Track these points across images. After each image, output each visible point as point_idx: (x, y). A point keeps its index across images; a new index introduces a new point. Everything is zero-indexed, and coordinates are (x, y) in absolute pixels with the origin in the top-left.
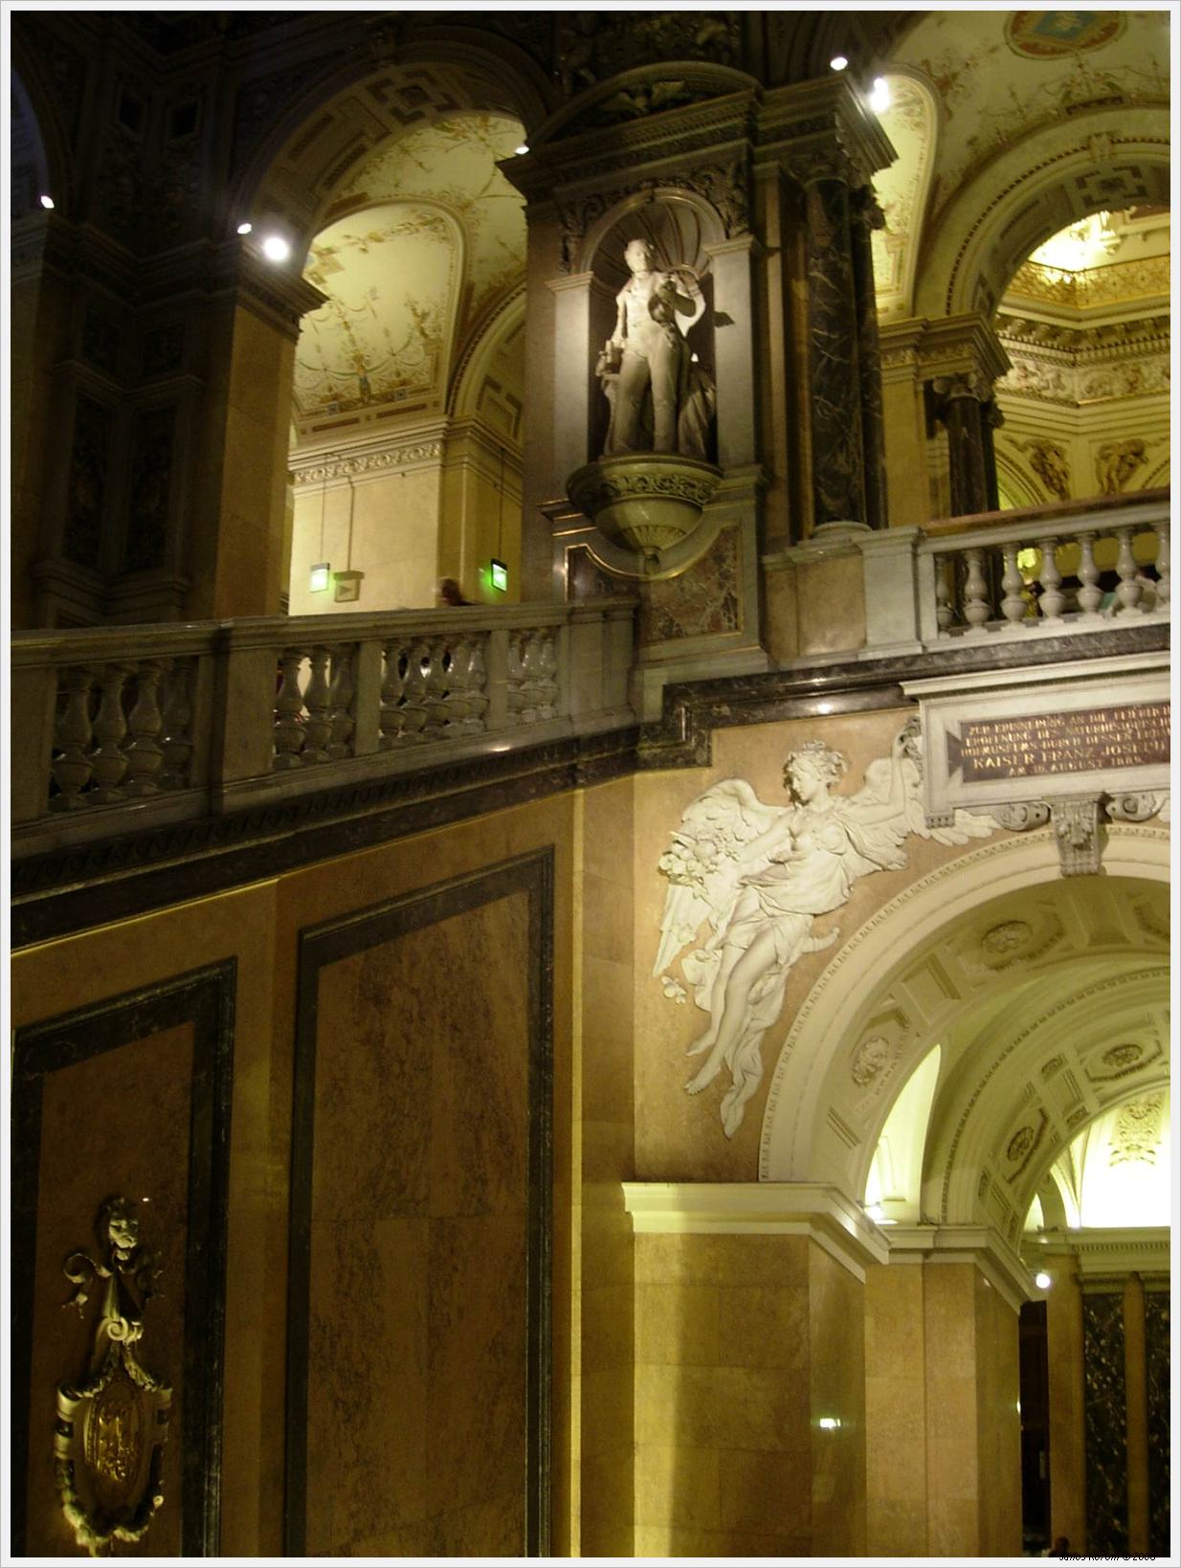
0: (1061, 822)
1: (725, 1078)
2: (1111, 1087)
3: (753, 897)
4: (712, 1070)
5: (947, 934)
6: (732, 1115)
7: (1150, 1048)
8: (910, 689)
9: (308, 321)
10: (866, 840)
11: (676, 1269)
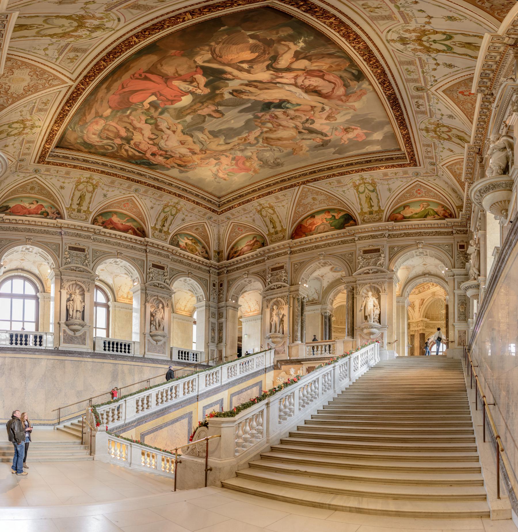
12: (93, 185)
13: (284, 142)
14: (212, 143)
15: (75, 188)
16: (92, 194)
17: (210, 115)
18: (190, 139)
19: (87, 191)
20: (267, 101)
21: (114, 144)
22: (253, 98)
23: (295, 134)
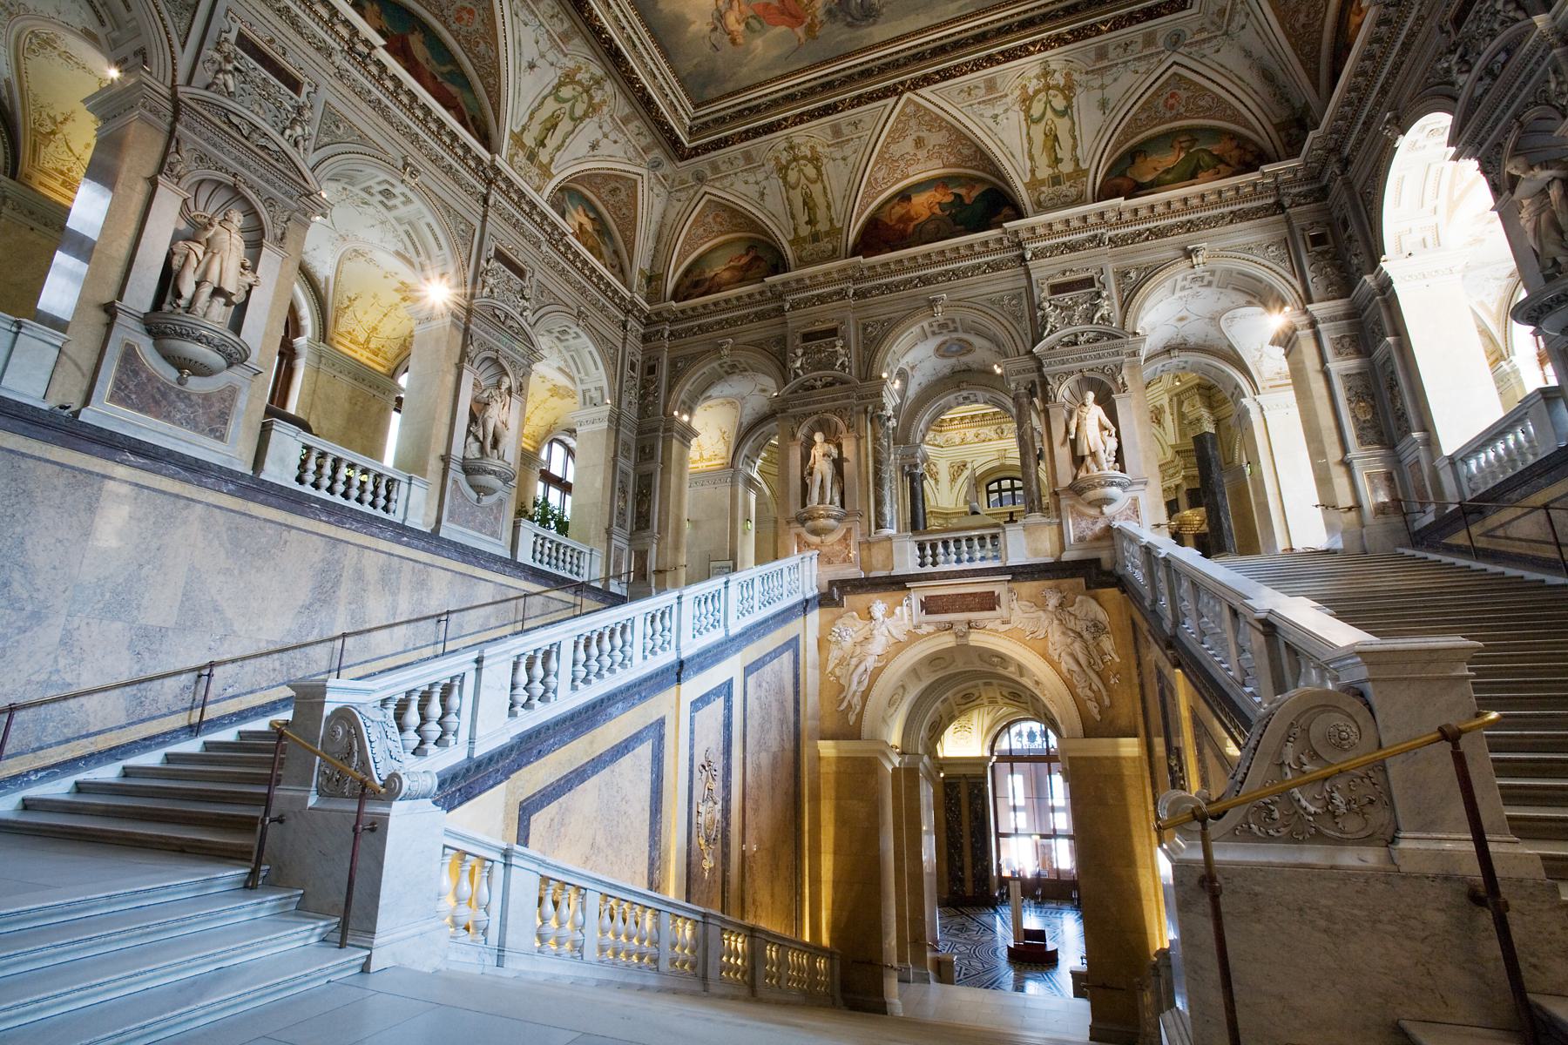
0: (957, 628)
1: (850, 705)
2: (963, 707)
3: (858, 650)
4: (845, 704)
5: (921, 662)
6: (852, 718)
7: (977, 695)
8: (908, 585)
9: (694, 441)
10: (894, 632)
11: (834, 768)
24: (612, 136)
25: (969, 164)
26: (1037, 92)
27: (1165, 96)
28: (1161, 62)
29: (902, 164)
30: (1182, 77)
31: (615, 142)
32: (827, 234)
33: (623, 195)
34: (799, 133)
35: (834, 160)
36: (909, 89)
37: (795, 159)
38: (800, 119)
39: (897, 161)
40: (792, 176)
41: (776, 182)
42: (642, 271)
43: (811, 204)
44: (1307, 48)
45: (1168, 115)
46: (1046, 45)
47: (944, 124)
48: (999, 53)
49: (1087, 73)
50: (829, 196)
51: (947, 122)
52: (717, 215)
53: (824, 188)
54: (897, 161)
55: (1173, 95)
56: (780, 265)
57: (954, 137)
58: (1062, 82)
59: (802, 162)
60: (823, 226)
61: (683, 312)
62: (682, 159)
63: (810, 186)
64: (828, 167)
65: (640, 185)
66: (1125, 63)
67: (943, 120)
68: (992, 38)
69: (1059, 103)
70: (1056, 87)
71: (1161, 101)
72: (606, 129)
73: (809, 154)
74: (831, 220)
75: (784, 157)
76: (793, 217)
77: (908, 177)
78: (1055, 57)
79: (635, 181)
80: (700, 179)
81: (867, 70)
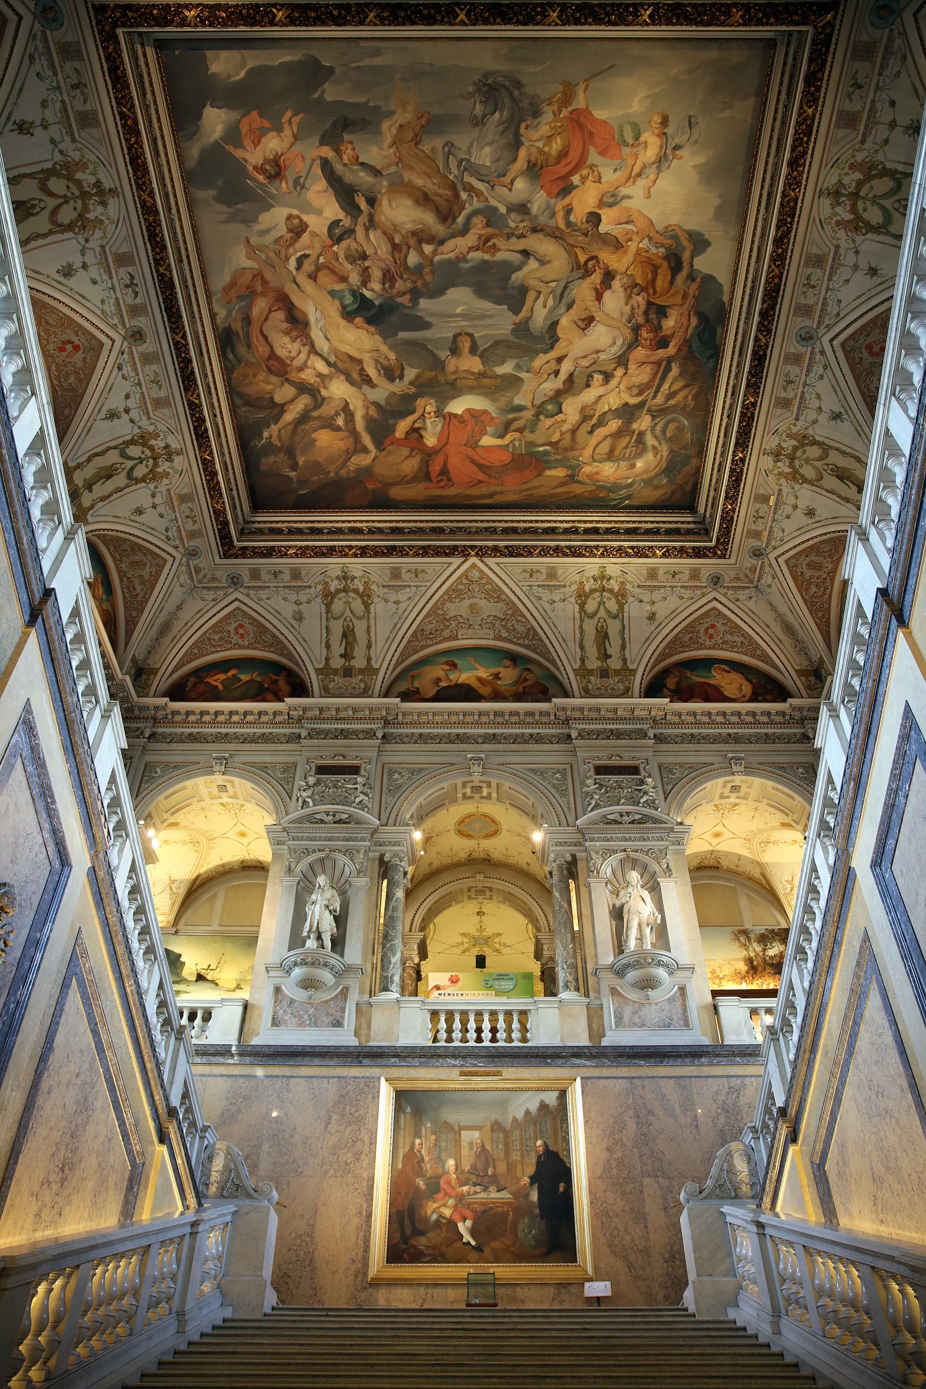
12: (803, 445)
13: (419, 181)
14: (545, 280)
15: (813, 485)
16: (831, 448)
17: (473, 350)
18: (564, 321)
19: (820, 459)
20: (372, 329)
21: (653, 429)
22: (384, 348)
23: (385, 202)
24: (161, 509)
25: (521, 641)
26: (592, 591)
27: (705, 626)
28: (704, 595)
29: (453, 624)
30: (720, 613)
31: (162, 516)
32: (361, 671)
33: (145, 573)
34: (357, 565)
35: (386, 601)
36: (477, 555)
37: (345, 590)
38: (363, 552)
39: (448, 620)
40: (338, 605)
41: (318, 607)
42: (134, 658)
43: (350, 640)
44: (820, 614)
45: (708, 643)
46: (606, 553)
47: (503, 597)
48: (567, 547)
49: (639, 586)
50: (372, 635)
51: (507, 596)
52: (241, 626)
53: (369, 627)
54: (448, 620)
55: (713, 626)
56: (300, 689)
57: (510, 612)
58: (616, 589)
59: (351, 594)
60: (359, 663)
61: (174, 713)
62: (227, 555)
63: (354, 620)
64: (378, 607)
65: (168, 566)
66: (672, 587)
67: (503, 592)
68: (560, 533)
69: (612, 606)
70: (611, 591)
71: (702, 629)
72: (158, 500)
73: (361, 589)
74: (369, 660)
75: (334, 586)
76: (328, 646)
77: (456, 638)
78: (614, 566)
79: (165, 561)
80: (235, 581)
81: (439, 528)
